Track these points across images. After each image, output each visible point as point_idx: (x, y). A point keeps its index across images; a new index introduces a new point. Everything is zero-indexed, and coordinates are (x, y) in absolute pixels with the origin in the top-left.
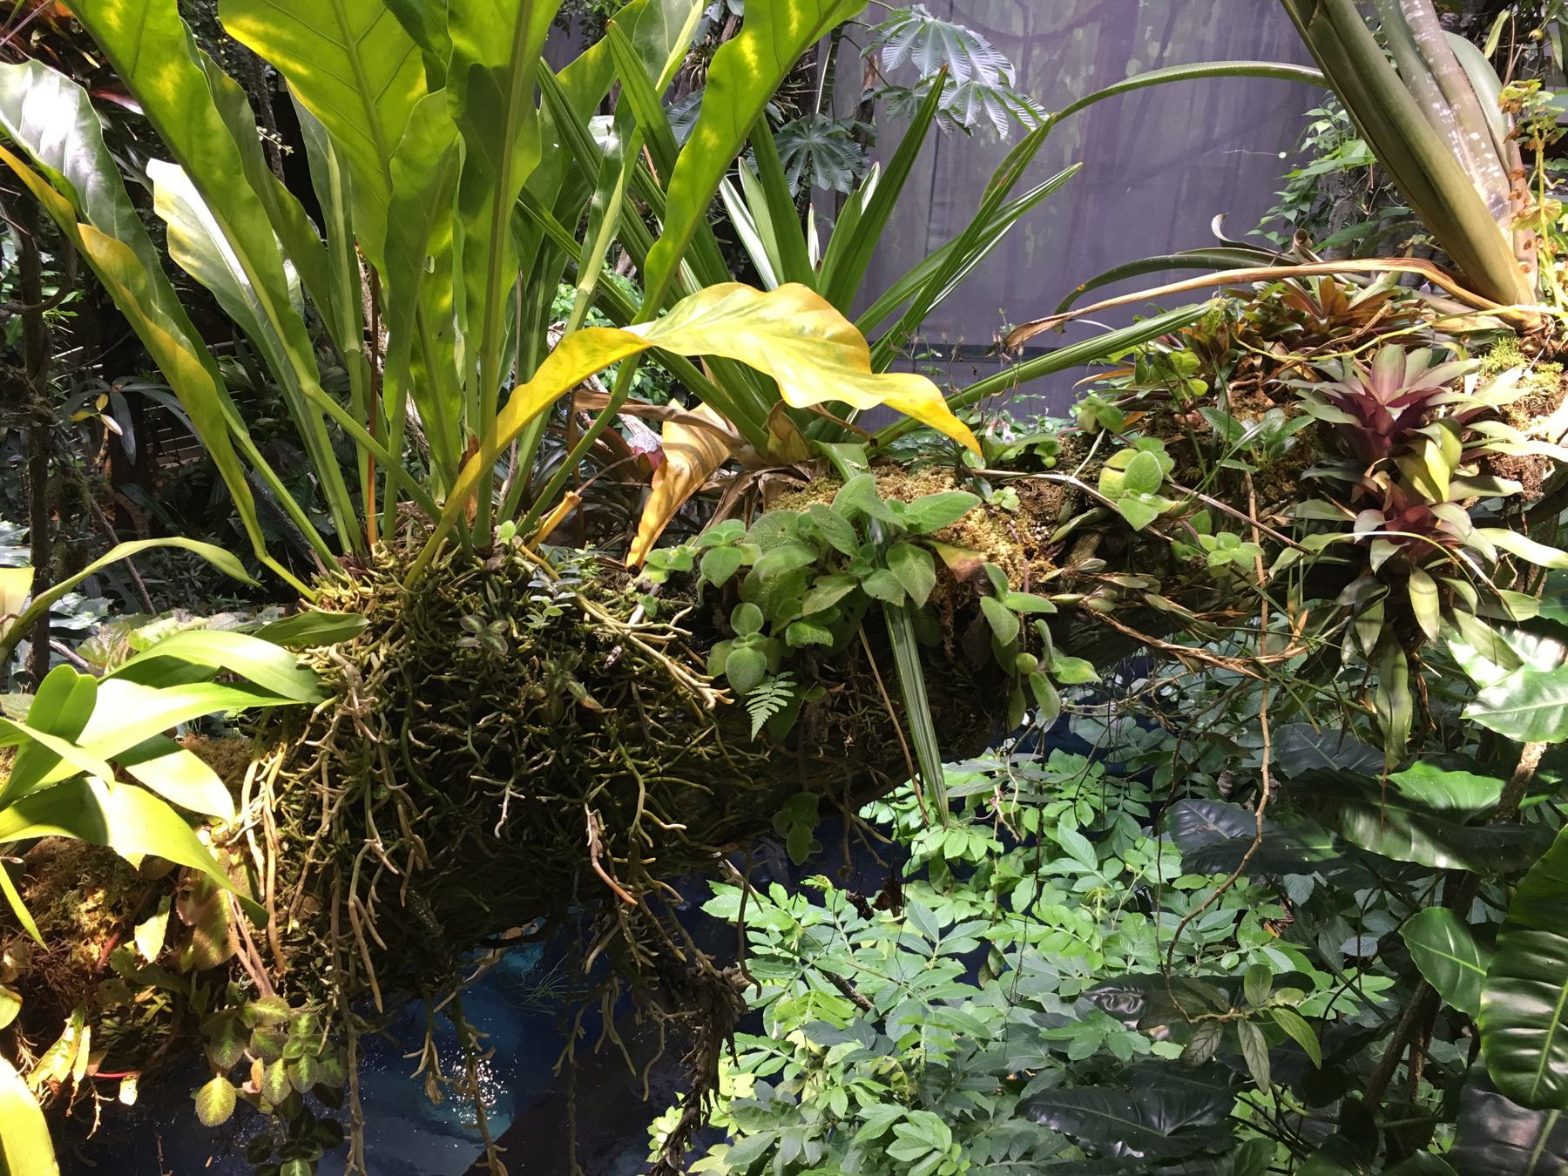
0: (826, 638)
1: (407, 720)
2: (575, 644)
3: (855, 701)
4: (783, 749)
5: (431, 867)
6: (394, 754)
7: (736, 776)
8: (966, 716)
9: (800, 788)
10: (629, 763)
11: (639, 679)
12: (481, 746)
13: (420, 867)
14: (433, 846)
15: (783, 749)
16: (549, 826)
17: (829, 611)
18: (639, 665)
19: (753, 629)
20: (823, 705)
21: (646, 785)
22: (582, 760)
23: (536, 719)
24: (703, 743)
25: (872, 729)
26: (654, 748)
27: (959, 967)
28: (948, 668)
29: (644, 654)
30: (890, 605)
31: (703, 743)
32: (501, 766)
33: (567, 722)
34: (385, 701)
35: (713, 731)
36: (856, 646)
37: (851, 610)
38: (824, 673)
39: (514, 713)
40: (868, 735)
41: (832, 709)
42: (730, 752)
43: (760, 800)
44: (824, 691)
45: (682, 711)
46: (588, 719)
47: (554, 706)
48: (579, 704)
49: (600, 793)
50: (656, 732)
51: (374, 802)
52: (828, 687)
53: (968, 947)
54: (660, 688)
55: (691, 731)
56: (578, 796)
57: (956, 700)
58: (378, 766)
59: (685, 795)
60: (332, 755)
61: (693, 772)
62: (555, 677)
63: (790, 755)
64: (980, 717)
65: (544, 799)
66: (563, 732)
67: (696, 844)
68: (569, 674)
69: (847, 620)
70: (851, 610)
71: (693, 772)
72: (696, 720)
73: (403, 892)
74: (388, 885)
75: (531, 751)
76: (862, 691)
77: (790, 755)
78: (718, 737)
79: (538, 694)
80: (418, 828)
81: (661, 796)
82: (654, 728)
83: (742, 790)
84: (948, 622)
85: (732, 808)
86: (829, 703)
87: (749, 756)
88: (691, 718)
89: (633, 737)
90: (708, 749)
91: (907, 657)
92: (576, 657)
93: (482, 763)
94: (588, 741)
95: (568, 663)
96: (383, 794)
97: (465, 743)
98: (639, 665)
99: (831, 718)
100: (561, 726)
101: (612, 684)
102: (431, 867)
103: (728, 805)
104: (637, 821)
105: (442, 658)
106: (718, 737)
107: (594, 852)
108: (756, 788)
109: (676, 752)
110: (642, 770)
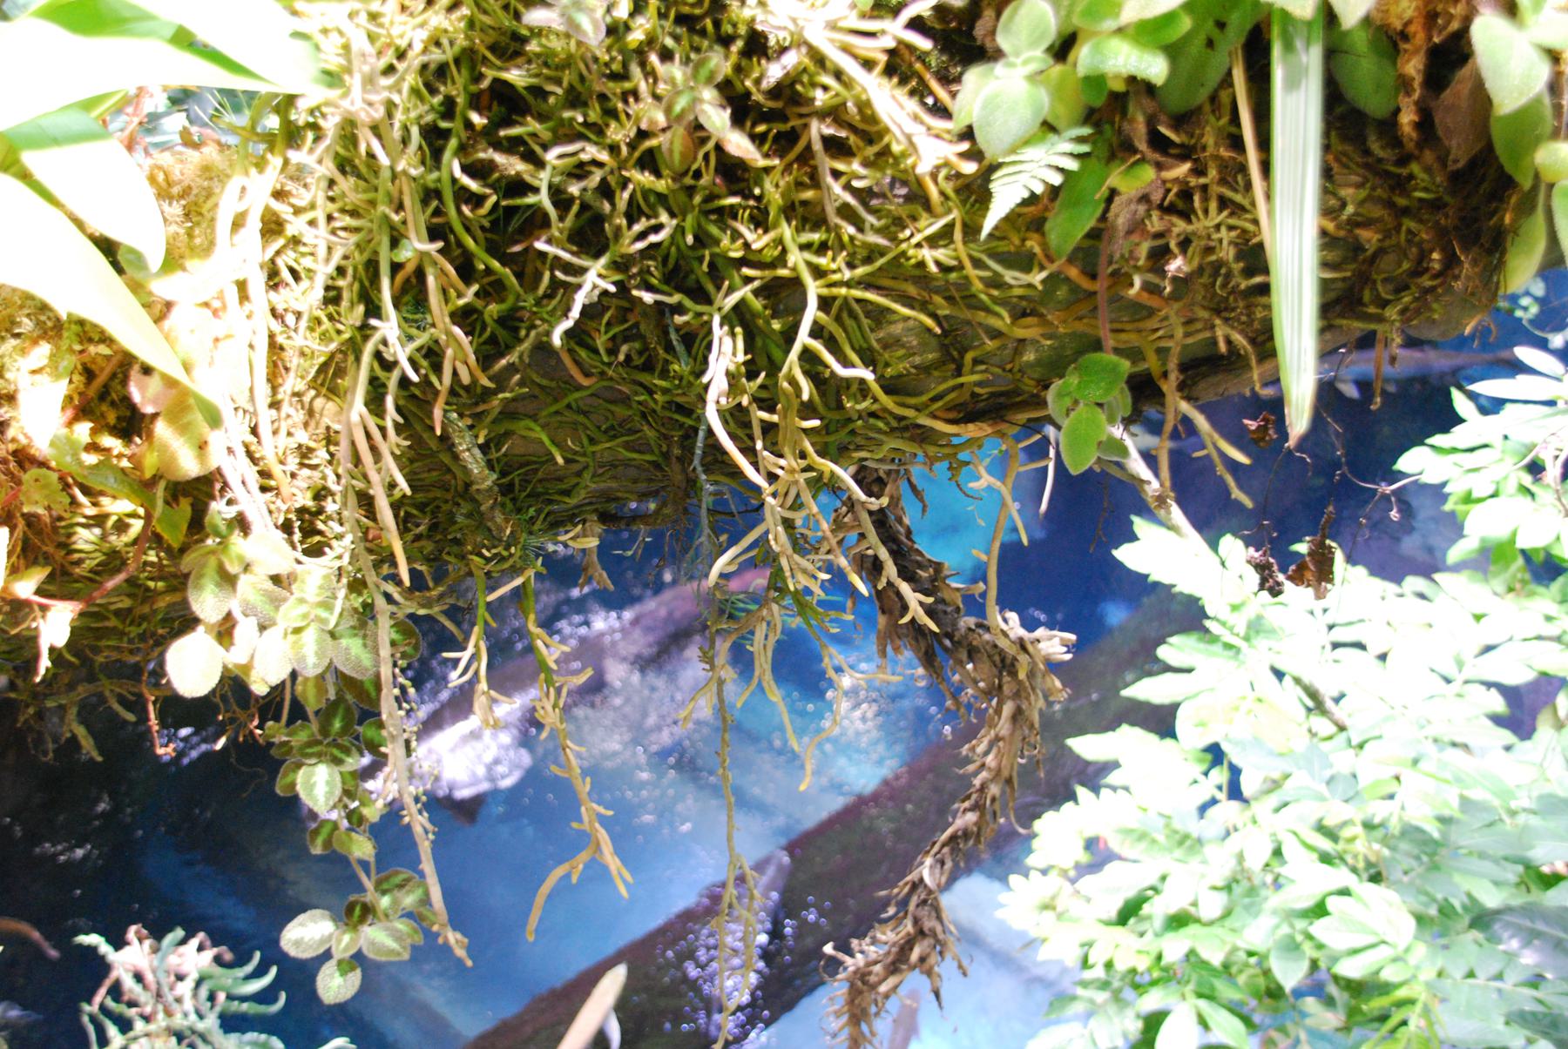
0: (1156, 68)
1: (453, 143)
2: (726, 41)
3: (1205, 199)
4: (1073, 273)
5: (485, 382)
6: (430, 195)
7: (988, 310)
8: (1423, 256)
9: (1097, 346)
10: (795, 257)
11: (823, 115)
12: (561, 200)
13: (465, 378)
14: (488, 354)
15: (1073, 273)
16: (648, 342)
17: (1169, 18)
18: (825, 88)
19: (1033, 44)
20: (1144, 198)
21: (825, 303)
22: (717, 242)
23: (649, 162)
24: (933, 241)
25: (1227, 253)
26: (839, 237)
27: (1498, 704)
28: (1404, 160)
29: (838, 75)
30: (1286, 16)
31: (933, 241)
32: (590, 236)
33: (698, 175)
34: (423, 108)
35: (949, 227)
36: (1224, 96)
37: (1221, 25)
38: (1158, 142)
39: (613, 149)
40: (1219, 264)
41: (1167, 210)
42: (977, 263)
43: (1029, 356)
44: (1148, 173)
45: (904, 183)
46: (734, 172)
47: (678, 148)
48: (719, 148)
49: (743, 301)
50: (845, 212)
51: (396, 267)
52: (1159, 167)
53: (1518, 676)
54: (870, 139)
55: (914, 219)
56: (709, 302)
57: (1409, 224)
58: (400, 207)
59: (897, 329)
60: (332, 183)
61: (912, 290)
62: (678, 93)
63: (1086, 284)
64: (1451, 261)
65: (648, 298)
66: (690, 191)
67: (909, 413)
68: (709, 94)
69: (1210, 43)
70: (1221, 25)
71: (912, 290)
72: (927, 205)
73: (438, 413)
74: (416, 400)
75: (632, 216)
76: (1223, 181)
77: (1086, 284)
78: (958, 235)
79: (652, 122)
80: (465, 317)
81: (849, 322)
82: (846, 205)
83: (995, 334)
84: (1413, 67)
85: (976, 362)
86: (1156, 197)
87: (1009, 276)
88: (918, 197)
89: (807, 216)
90: (942, 254)
91: (1298, 113)
92: (721, 63)
93: (558, 228)
94: (733, 212)
95: (704, 73)
96: (406, 254)
97: (536, 190)
98: (825, 88)
99: (1156, 223)
100: (688, 181)
101: (785, 119)
102: (485, 382)
103: (969, 356)
104: (794, 355)
105: (511, 46)
106: (958, 235)
107: (711, 396)
108: (1020, 333)
109: (879, 252)
110: (818, 273)
